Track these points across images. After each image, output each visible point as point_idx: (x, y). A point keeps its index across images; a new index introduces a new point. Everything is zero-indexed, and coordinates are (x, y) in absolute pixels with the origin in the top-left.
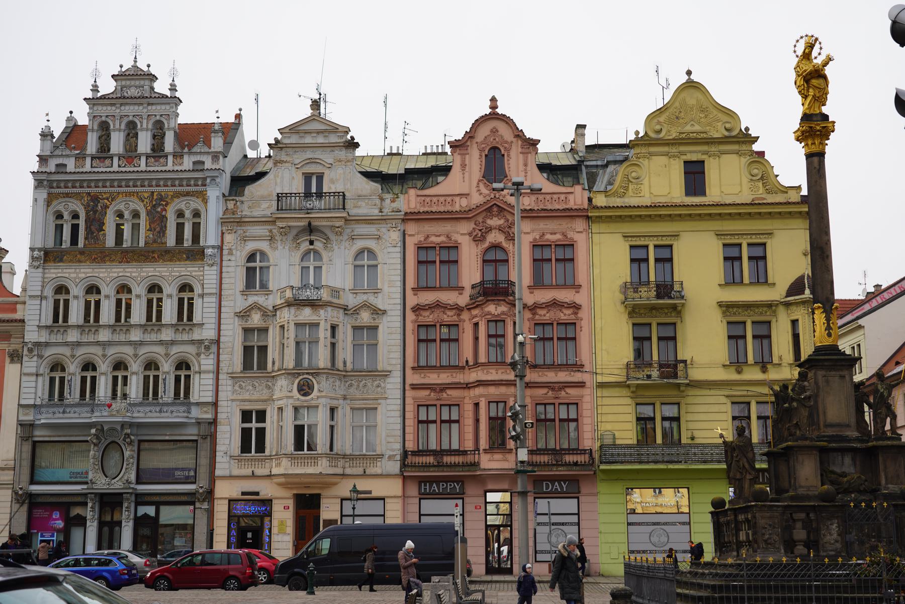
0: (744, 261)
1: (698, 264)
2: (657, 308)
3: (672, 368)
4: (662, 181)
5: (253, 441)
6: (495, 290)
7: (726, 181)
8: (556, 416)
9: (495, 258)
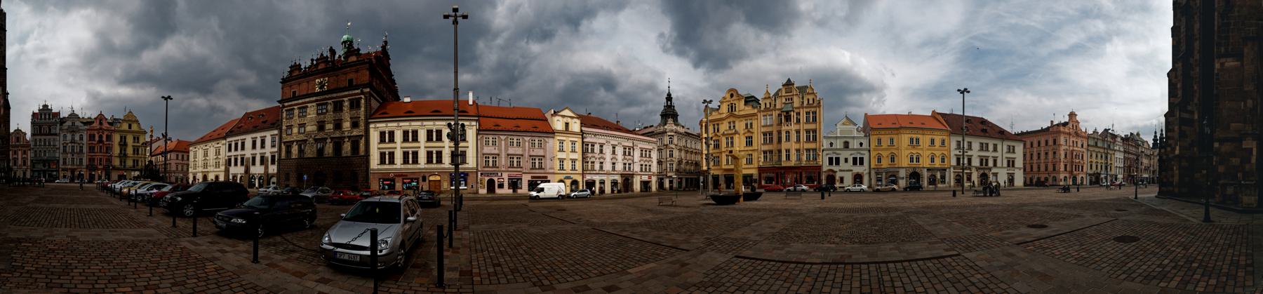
0: (136, 139)
1: (130, 140)
2: (123, 144)
3: (125, 155)
4: (125, 126)
5: (65, 163)
6: (101, 141)
7: (135, 127)
8: (109, 160)
9: (101, 137)
